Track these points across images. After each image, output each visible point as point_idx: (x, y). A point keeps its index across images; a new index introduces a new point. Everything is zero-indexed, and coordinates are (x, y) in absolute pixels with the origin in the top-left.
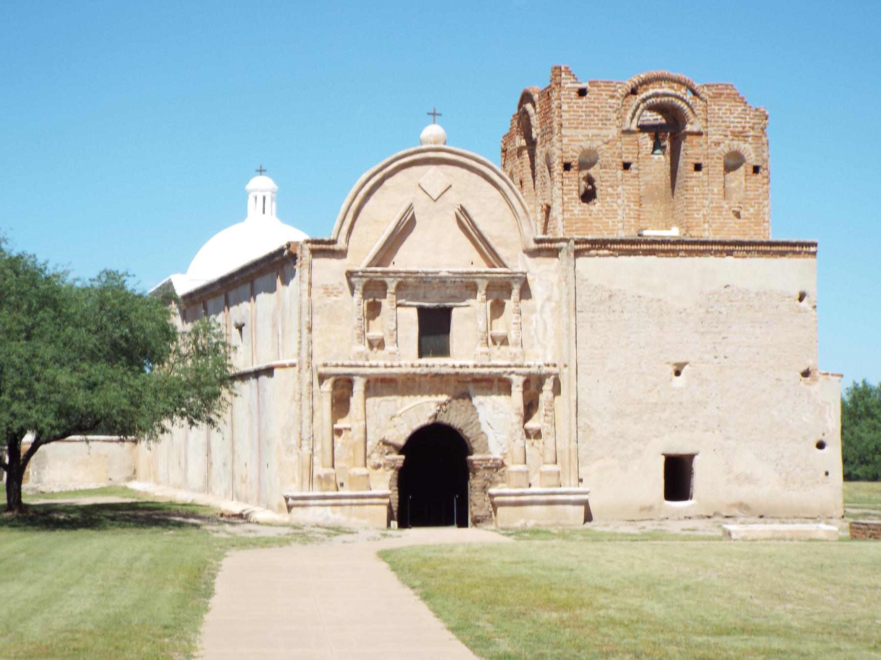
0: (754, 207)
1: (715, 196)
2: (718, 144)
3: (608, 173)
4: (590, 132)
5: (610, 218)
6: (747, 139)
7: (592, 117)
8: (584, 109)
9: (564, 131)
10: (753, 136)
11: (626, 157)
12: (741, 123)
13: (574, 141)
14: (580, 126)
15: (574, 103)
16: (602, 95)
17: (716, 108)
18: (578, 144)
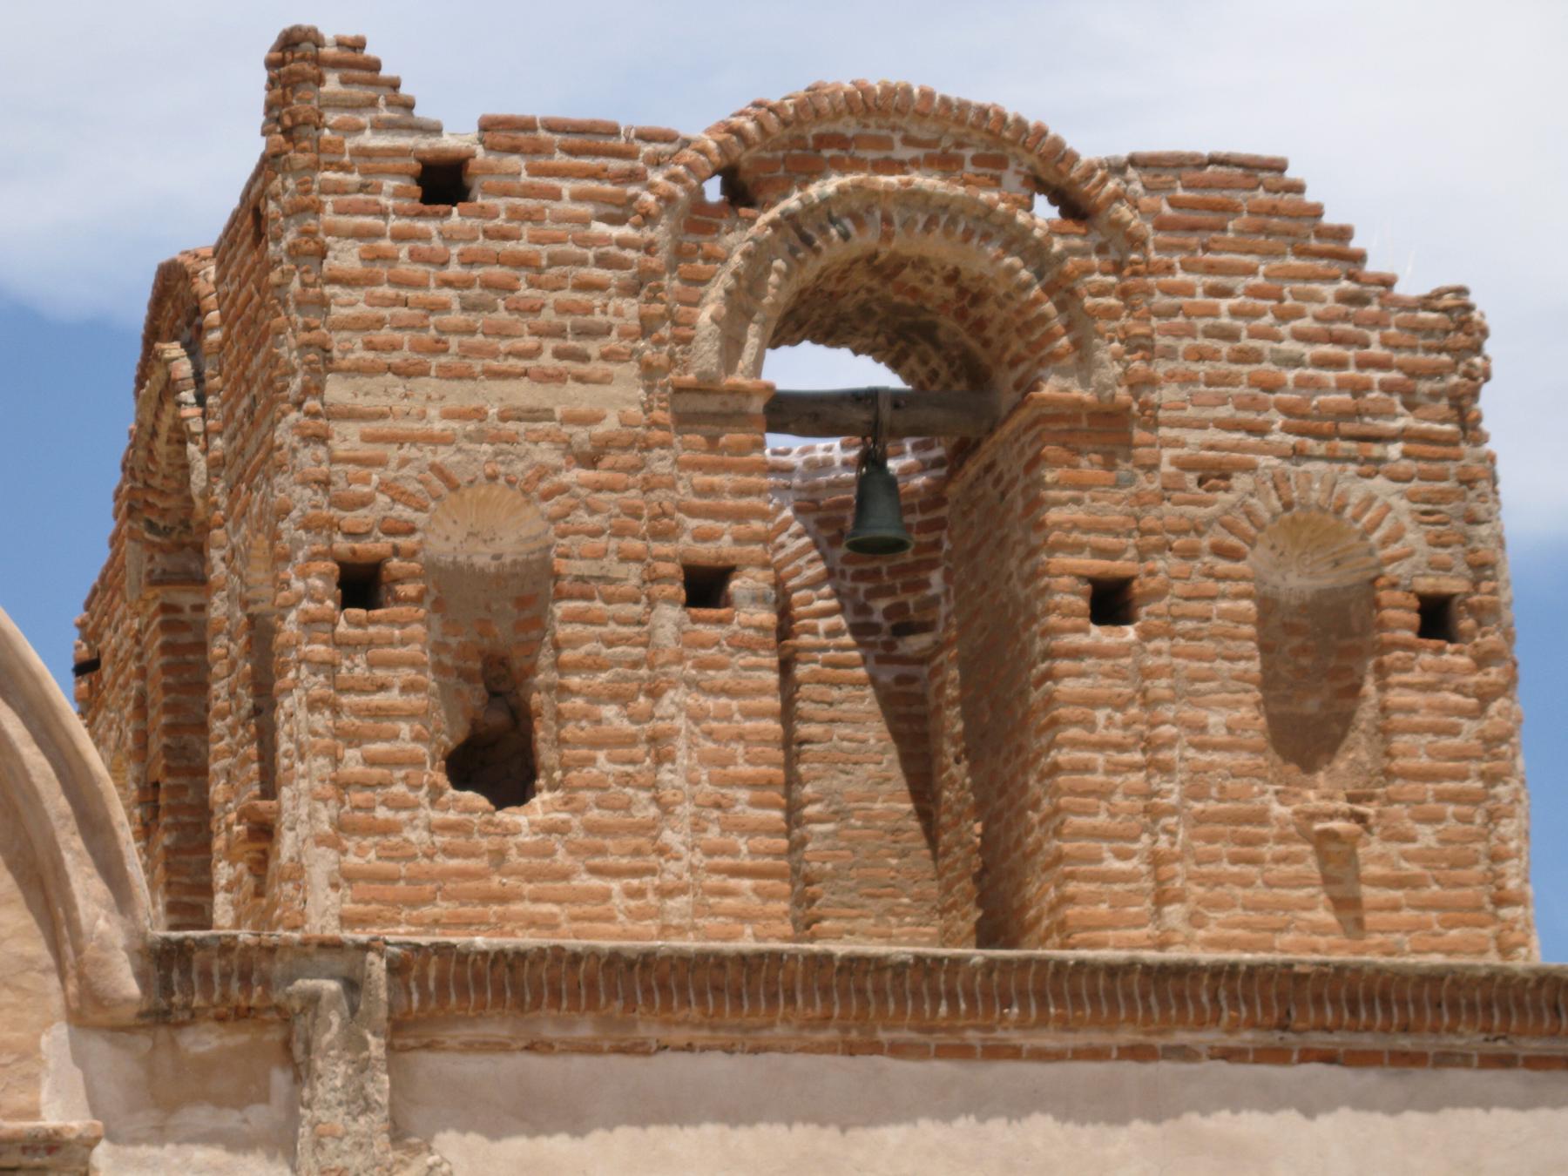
0: (1434, 819)
1: (1205, 758)
2: (1214, 474)
3: (600, 621)
4: (493, 396)
5: (617, 873)
6: (1376, 450)
7: (502, 316)
8: (454, 270)
9: (337, 391)
10: (1403, 435)
11: (703, 537)
12: (1340, 364)
13: (399, 440)
14: (434, 362)
15: (399, 237)
16: (556, 195)
17: (1199, 281)
18: (428, 454)
